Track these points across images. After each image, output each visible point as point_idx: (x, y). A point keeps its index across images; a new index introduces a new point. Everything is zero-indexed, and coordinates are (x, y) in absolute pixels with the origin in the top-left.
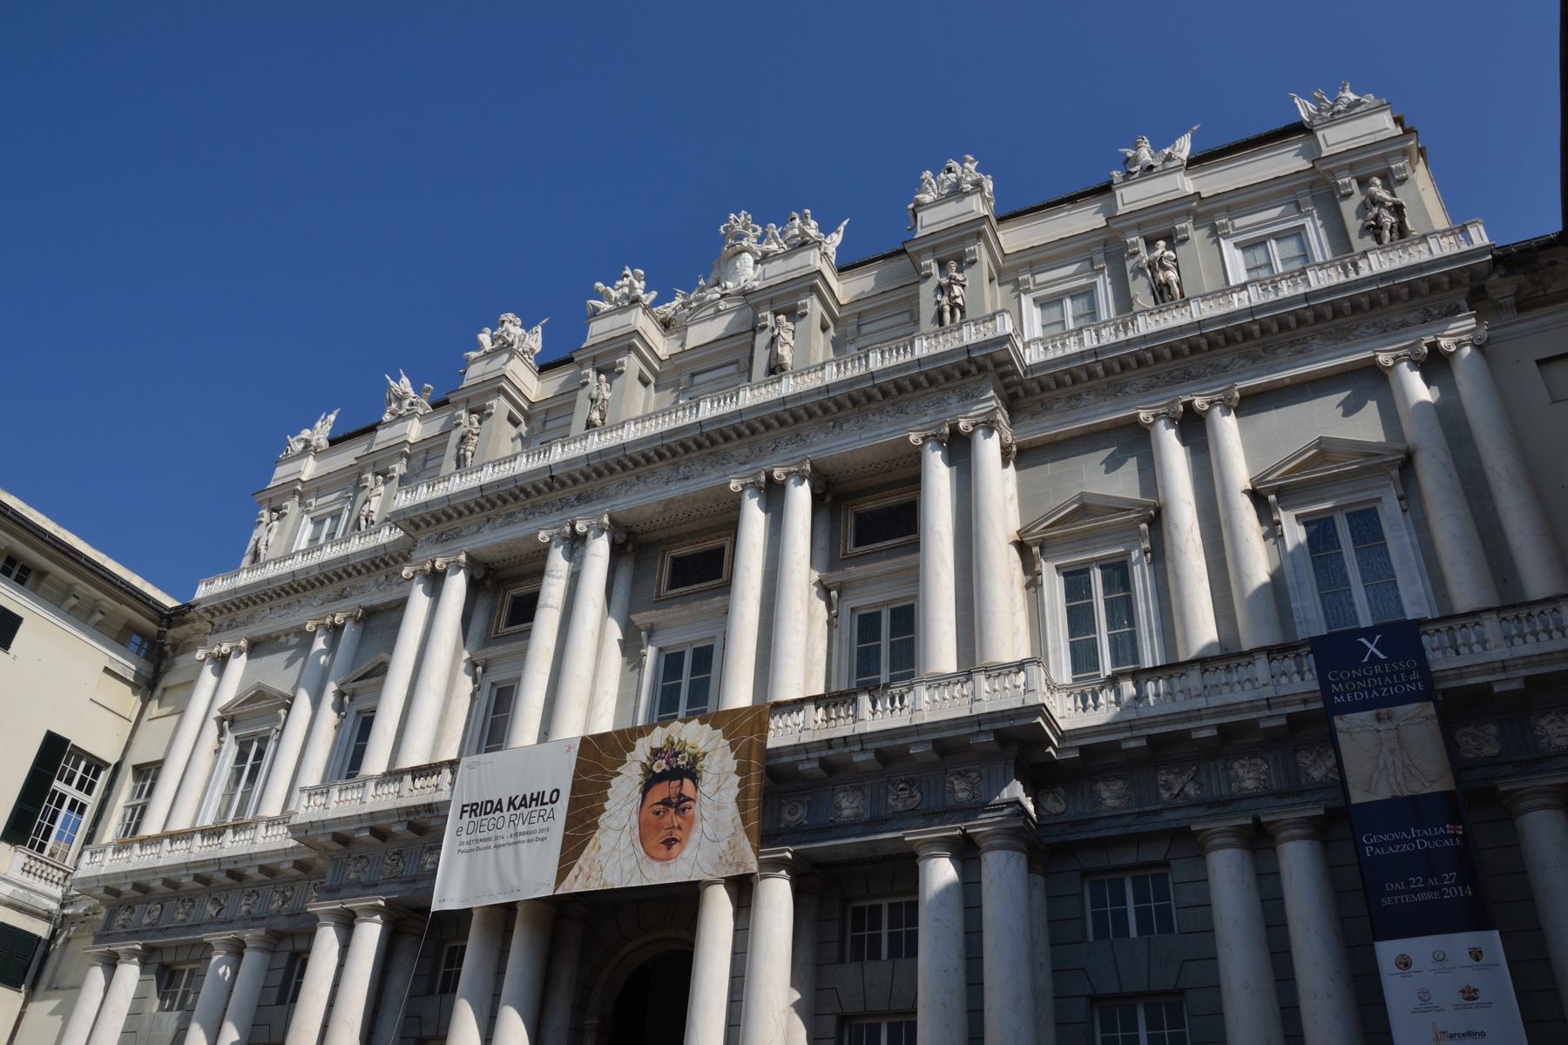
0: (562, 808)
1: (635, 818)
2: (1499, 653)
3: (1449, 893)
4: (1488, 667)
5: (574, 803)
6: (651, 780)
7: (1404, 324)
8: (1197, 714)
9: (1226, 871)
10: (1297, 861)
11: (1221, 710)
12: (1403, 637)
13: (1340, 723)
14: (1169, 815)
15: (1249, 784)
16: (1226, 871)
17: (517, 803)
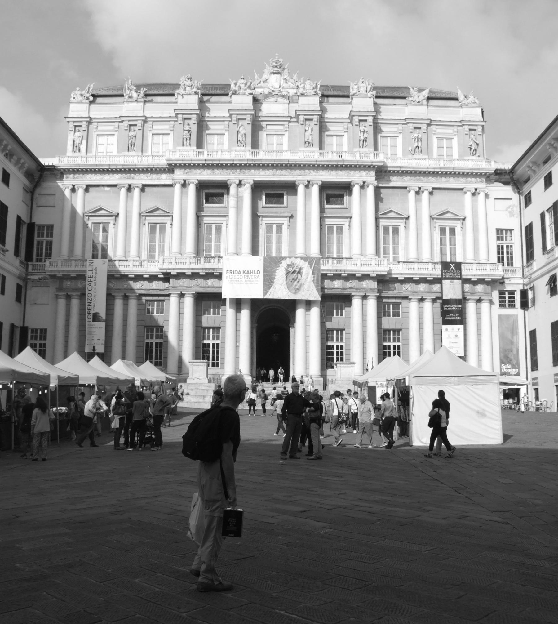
0: (261, 275)
1: (285, 282)
2: (475, 272)
3: (457, 318)
4: (472, 275)
5: (265, 276)
6: (288, 273)
7: (471, 181)
8: (416, 274)
9: (413, 306)
10: (428, 306)
11: (421, 274)
12: (458, 266)
13: (444, 281)
14: (404, 293)
15: (421, 289)
16: (413, 306)
17: (246, 272)
